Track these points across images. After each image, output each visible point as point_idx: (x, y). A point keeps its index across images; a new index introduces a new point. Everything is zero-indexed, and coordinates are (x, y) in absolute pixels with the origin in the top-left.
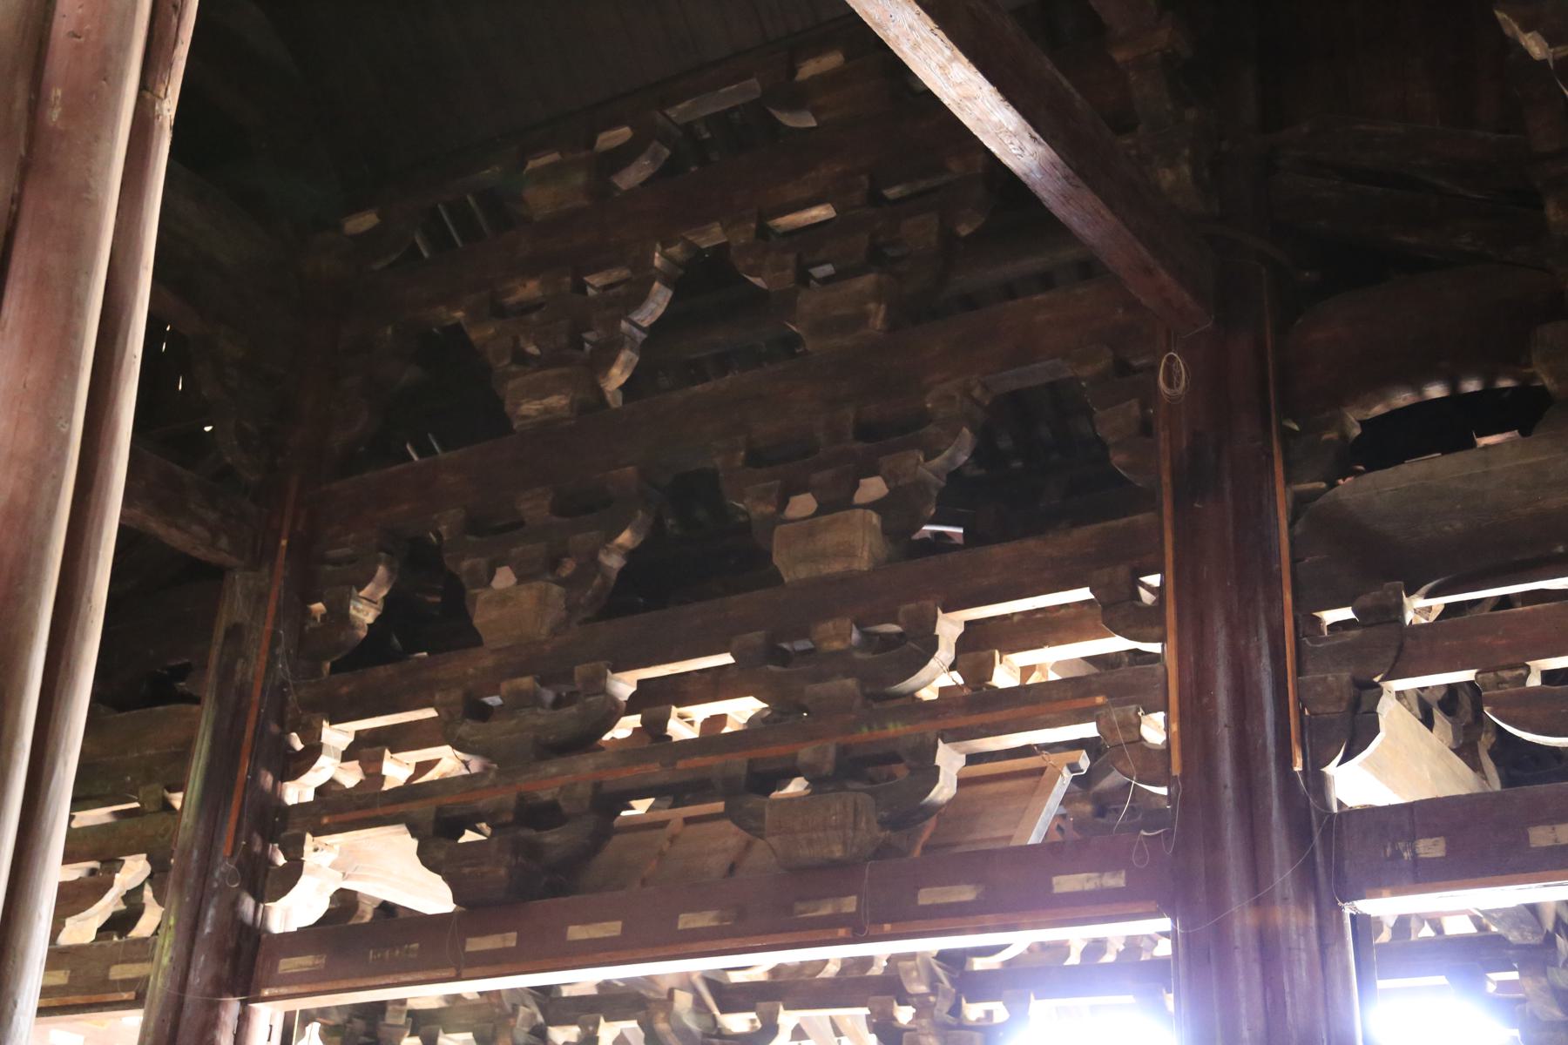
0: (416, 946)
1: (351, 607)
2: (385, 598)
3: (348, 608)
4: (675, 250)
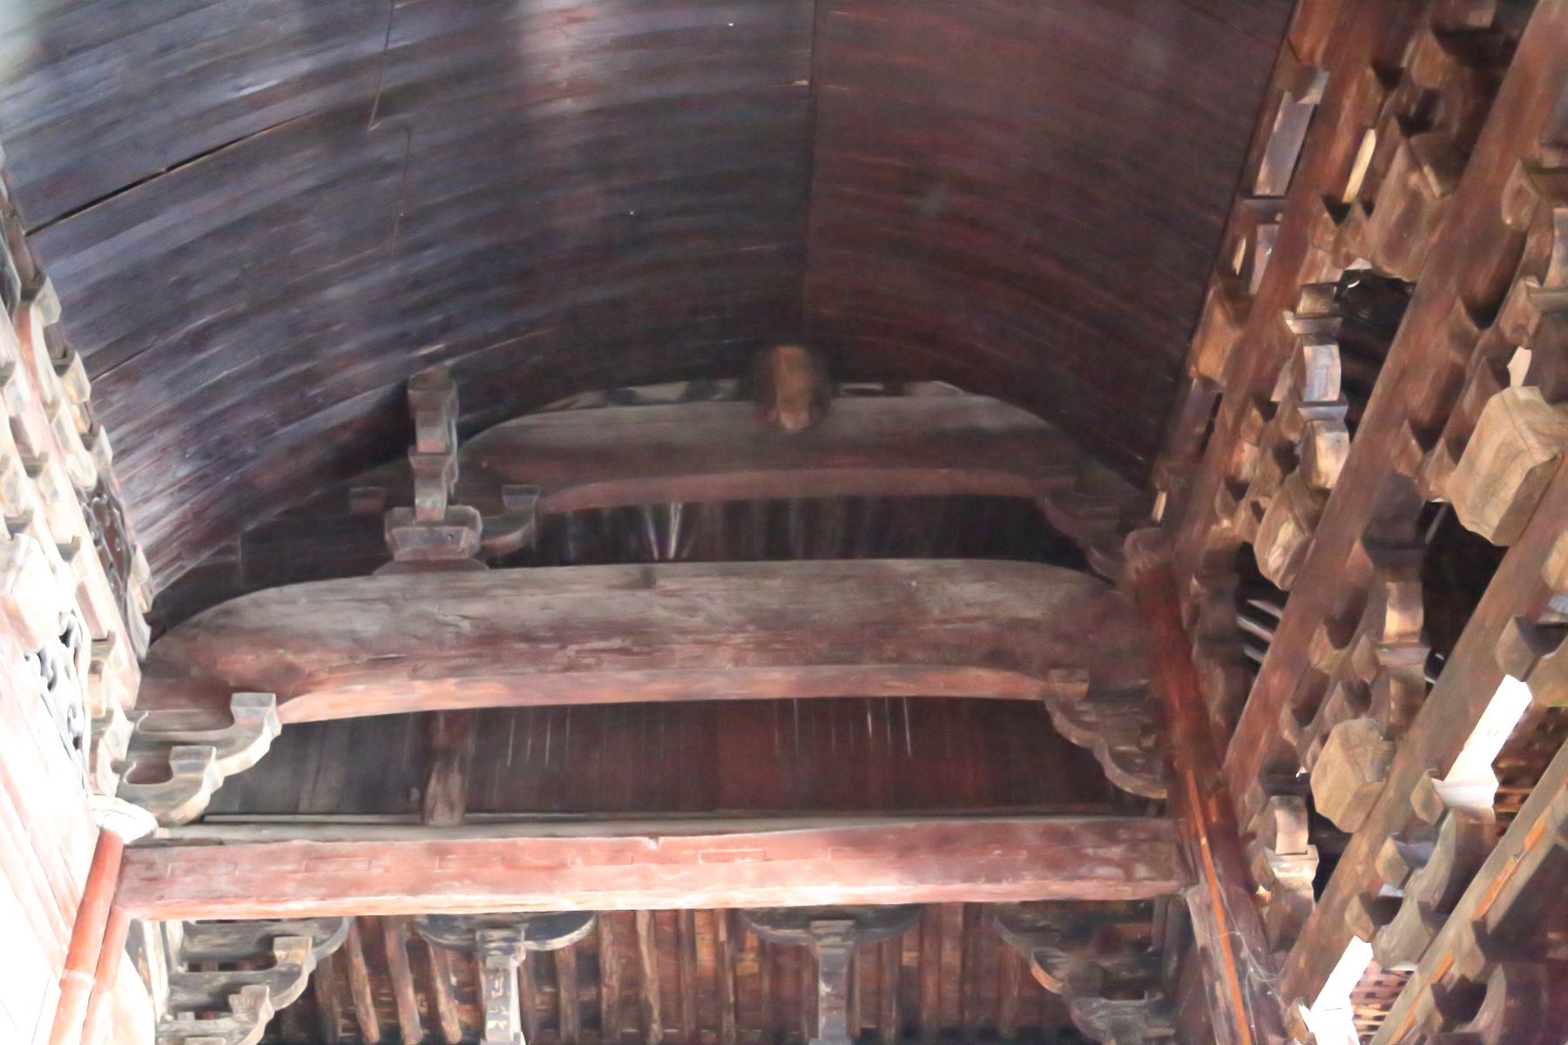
1: (1275, 870)
2: (1310, 842)
4: (1305, 305)
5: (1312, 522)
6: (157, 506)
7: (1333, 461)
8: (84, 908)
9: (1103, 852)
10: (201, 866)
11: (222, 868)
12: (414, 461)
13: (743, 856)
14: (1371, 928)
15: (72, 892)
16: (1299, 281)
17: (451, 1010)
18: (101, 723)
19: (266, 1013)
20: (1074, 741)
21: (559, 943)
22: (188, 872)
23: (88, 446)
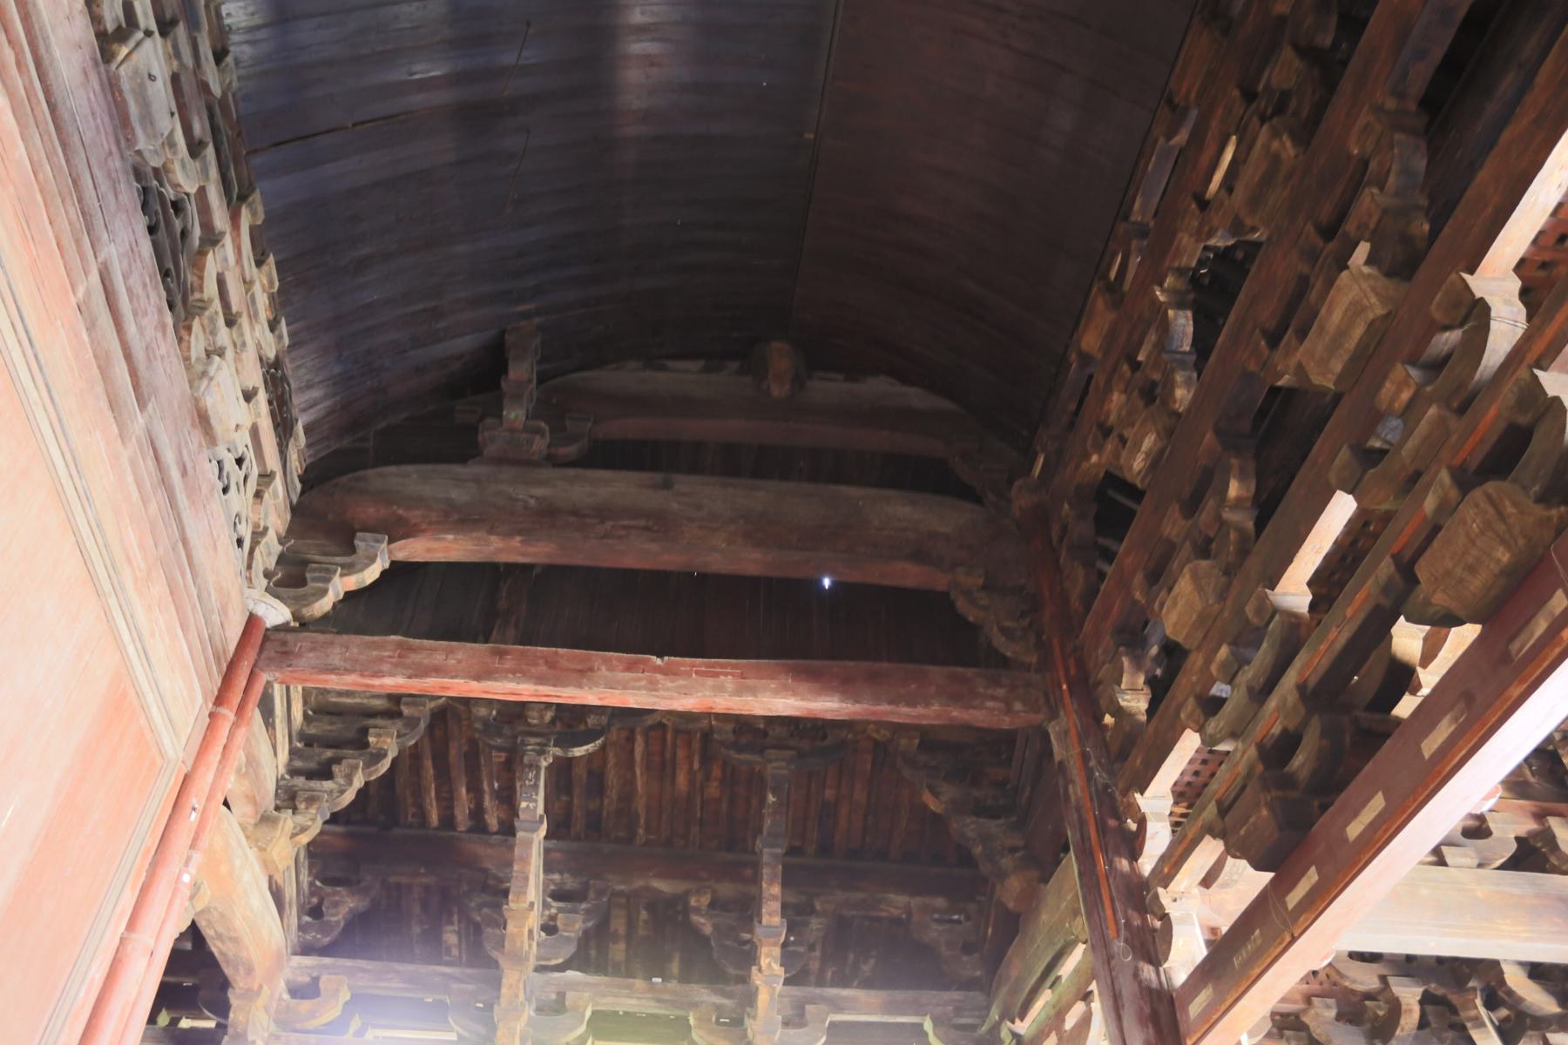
0: (1257, 932)
1: (1120, 700)
3: (1118, 702)
4: (1169, 281)
5: (1168, 434)
6: (316, 393)
7: (1185, 392)
8: (232, 666)
9: (990, 691)
10: (322, 647)
11: (337, 650)
12: (504, 385)
13: (726, 674)
14: (1202, 718)
15: (224, 651)
16: (1167, 264)
17: (493, 807)
18: (259, 534)
19: (358, 781)
20: (971, 619)
21: (578, 752)
22: (312, 650)
23: (272, 329)
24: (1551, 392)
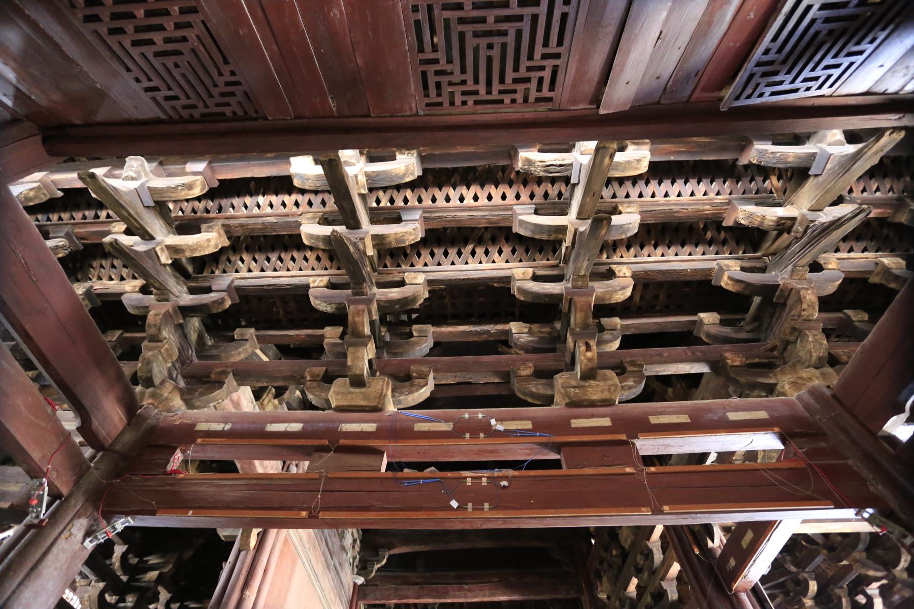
8: (352, 601)
24: (665, 588)
